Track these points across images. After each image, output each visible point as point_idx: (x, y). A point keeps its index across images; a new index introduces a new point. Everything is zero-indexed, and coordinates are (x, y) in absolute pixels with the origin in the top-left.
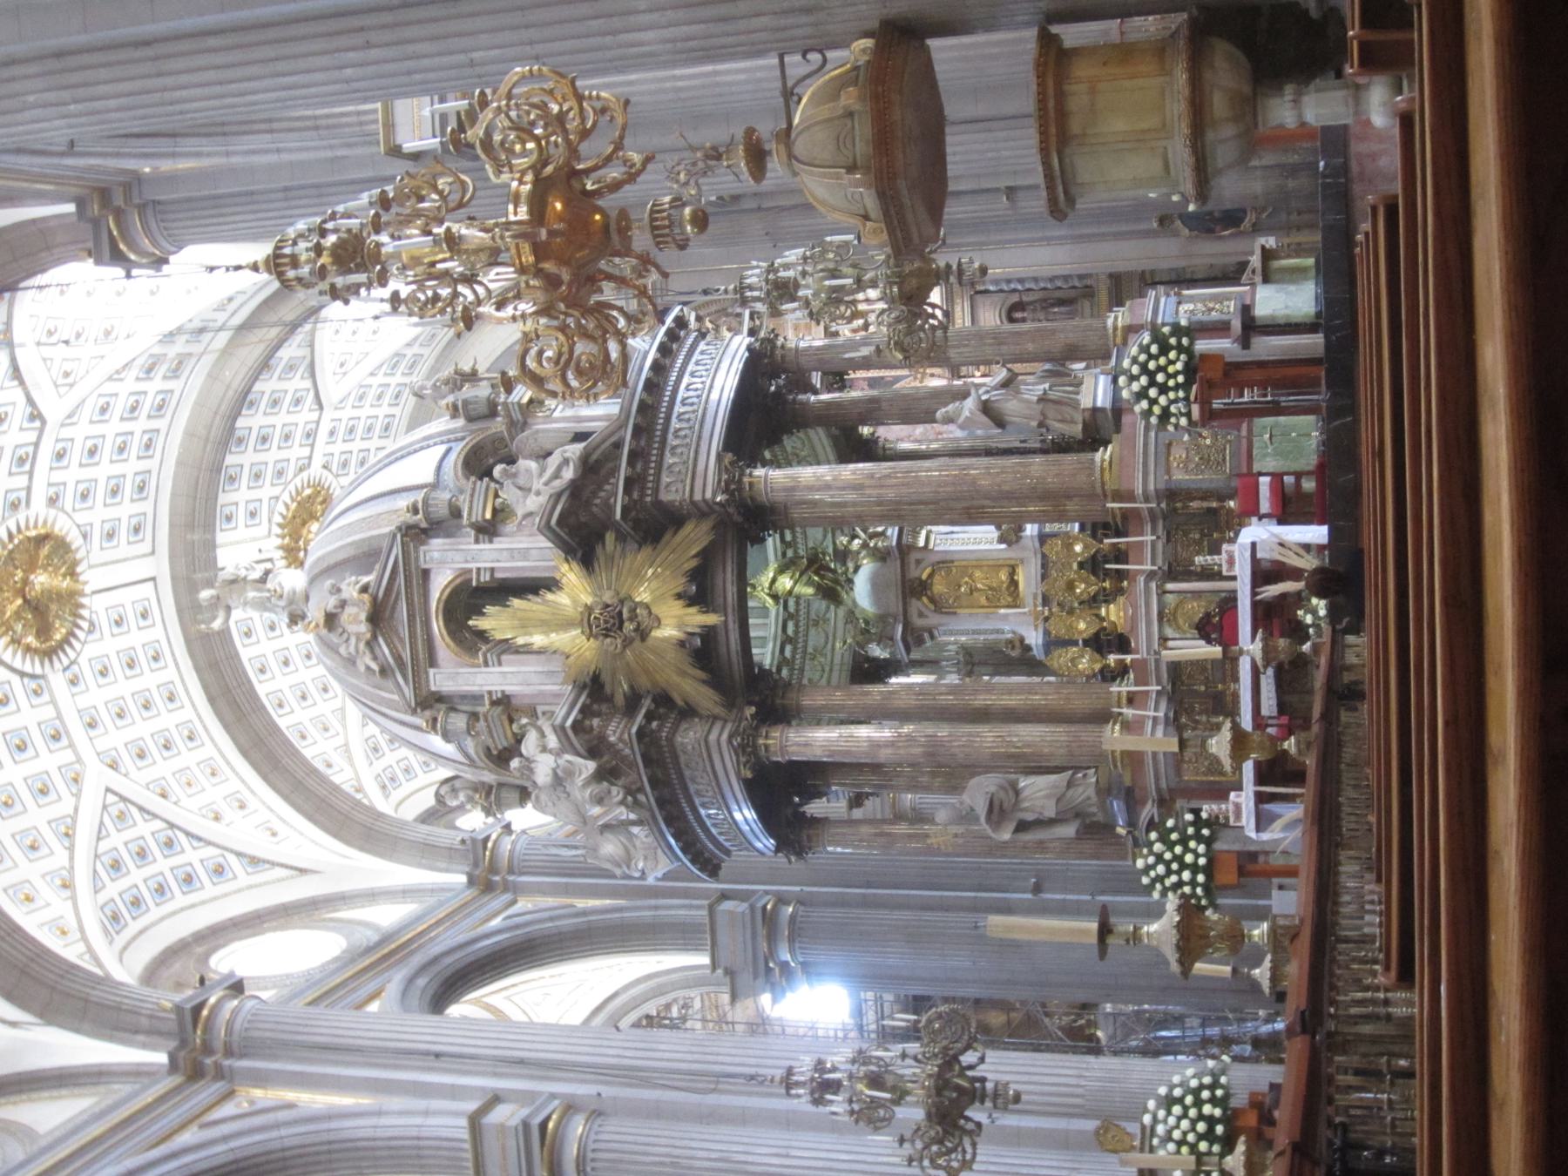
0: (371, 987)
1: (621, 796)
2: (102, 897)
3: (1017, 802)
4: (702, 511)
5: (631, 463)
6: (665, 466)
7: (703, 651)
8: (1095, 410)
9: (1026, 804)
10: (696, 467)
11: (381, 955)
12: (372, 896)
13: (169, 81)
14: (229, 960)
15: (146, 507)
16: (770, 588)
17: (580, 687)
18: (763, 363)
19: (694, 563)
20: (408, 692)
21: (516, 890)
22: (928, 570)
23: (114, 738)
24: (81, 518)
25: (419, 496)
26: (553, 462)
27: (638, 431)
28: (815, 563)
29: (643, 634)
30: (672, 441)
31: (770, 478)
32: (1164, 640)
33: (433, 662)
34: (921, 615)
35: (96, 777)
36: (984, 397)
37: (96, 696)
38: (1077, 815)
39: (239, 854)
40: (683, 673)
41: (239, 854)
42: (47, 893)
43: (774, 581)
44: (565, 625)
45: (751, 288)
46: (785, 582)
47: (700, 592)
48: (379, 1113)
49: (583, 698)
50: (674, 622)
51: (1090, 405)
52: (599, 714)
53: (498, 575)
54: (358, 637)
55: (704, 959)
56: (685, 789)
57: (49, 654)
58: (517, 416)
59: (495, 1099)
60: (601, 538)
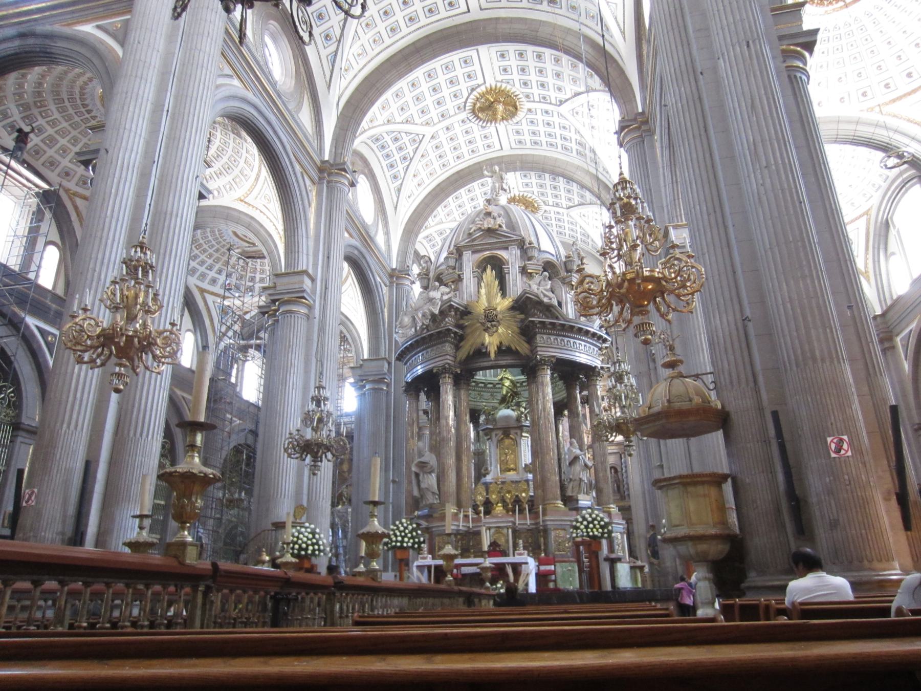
0: (354, 234)
2: (385, 135)
4: (533, 350)
5: (551, 323)
7: (480, 353)
8: (577, 500)
10: (550, 348)
11: (366, 238)
12: (387, 234)
13: (692, 141)
14: (363, 183)
15: (529, 145)
17: (466, 307)
18: (590, 372)
19: (513, 348)
20: (462, 244)
21: (391, 287)
23: (443, 137)
24: (524, 121)
25: (536, 245)
26: (550, 294)
27: (563, 325)
28: (515, 394)
29: (486, 330)
30: (559, 339)
31: (547, 376)
32: (489, 528)
33: (474, 252)
35: (428, 131)
37: (458, 129)
38: (422, 496)
39: (401, 184)
40: (471, 346)
41: (401, 184)
42: (386, 115)
44: (489, 301)
45: (620, 365)
46: (507, 383)
47: (503, 351)
48: (307, 238)
50: (491, 341)
52: (456, 314)
54: (483, 225)
55: (366, 357)
56: (428, 347)
57: (473, 112)
58: (567, 280)
59: (313, 280)
60: (521, 314)
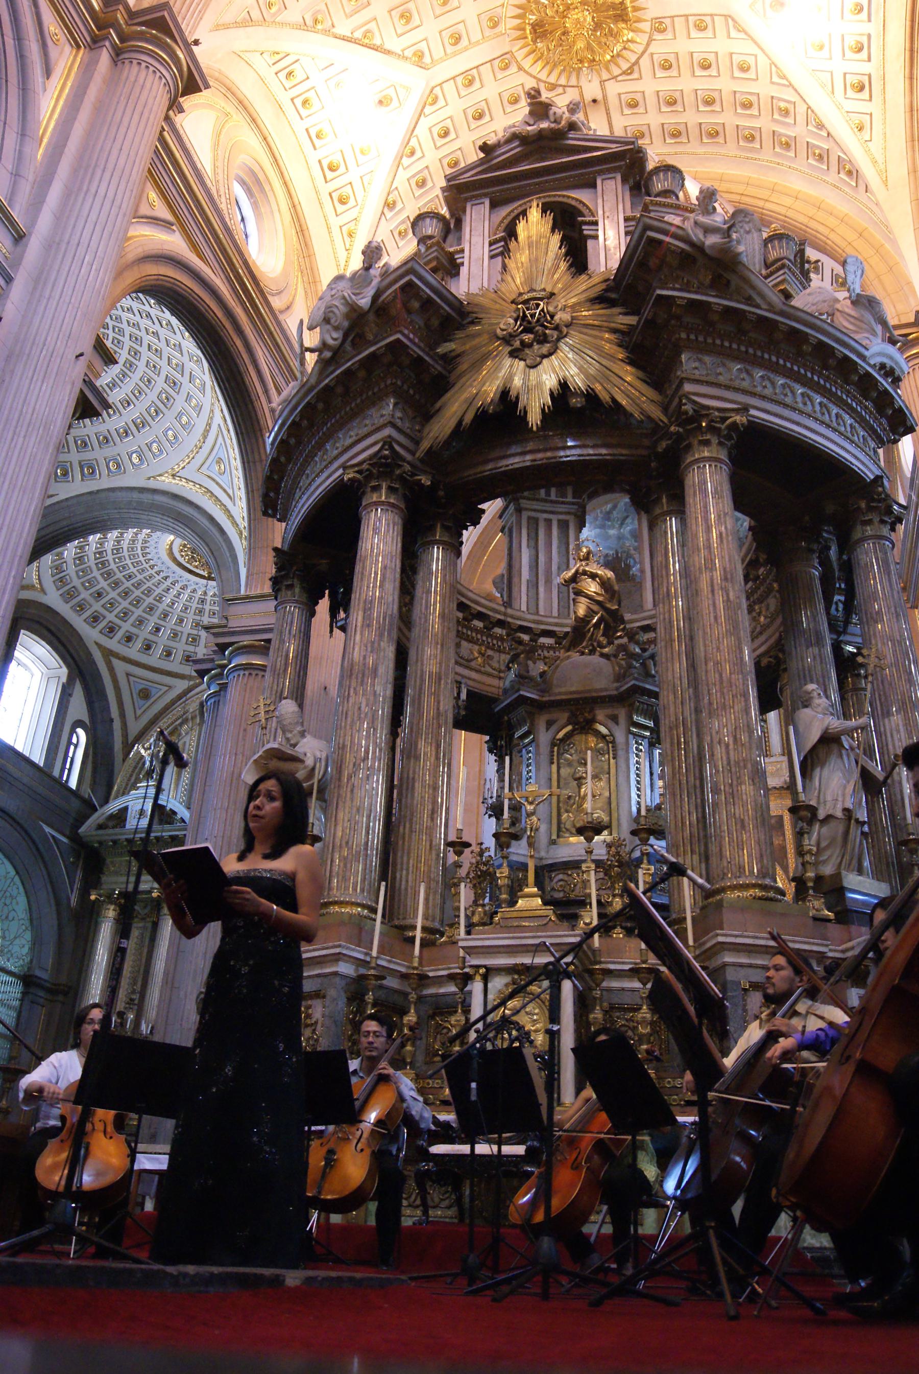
1: (330, 342)
6: (727, 362)
16: (585, 573)
19: (604, 396)
22: (603, 730)
24: (645, 62)
32: (488, 974)
34: (549, 724)
43: (593, 576)
46: (592, 587)
49: (447, 308)
51: (846, 884)
53: (590, 243)
55: (243, 592)
59: (19, 237)
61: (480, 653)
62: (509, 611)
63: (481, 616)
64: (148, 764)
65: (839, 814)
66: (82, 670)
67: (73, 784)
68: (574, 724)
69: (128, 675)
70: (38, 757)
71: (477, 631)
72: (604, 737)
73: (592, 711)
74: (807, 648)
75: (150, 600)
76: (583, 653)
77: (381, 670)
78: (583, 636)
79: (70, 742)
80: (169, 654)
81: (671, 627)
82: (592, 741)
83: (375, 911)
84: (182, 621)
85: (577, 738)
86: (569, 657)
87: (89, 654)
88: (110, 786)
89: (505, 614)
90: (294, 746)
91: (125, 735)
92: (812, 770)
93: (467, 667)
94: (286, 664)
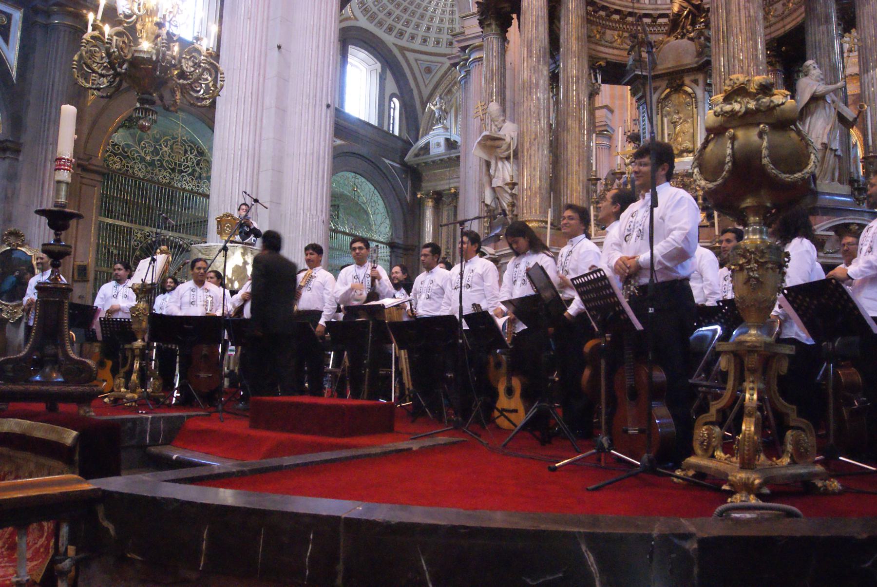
3: (501, 159)
9: (500, 164)
22: (689, 90)
36: (829, 100)
61: (619, 36)
62: (636, 5)
63: (617, 12)
64: (437, 115)
65: (819, 147)
66: (389, 63)
67: (397, 133)
68: (671, 88)
69: (416, 60)
70: (374, 121)
71: (616, 22)
72: (690, 94)
73: (682, 77)
74: (819, 26)
75: (421, 11)
76: (677, 38)
77: (541, 82)
78: (678, 25)
79: (390, 107)
80: (438, 43)
81: (719, 30)
82: (683, 98)
83: (546, 222)
84: (442, 21)
85: (674, 97)
86: (668, 42)
87: (390, 51)
88: (417, 130)
89: (633, 8)
90: (500, 129)
91: (421, 97)
92: (806, 117)
93: (610, 47)
94: (492, 76)
